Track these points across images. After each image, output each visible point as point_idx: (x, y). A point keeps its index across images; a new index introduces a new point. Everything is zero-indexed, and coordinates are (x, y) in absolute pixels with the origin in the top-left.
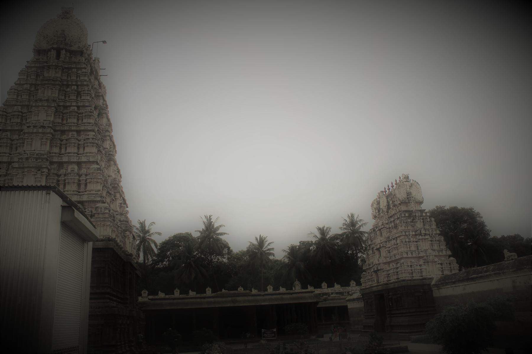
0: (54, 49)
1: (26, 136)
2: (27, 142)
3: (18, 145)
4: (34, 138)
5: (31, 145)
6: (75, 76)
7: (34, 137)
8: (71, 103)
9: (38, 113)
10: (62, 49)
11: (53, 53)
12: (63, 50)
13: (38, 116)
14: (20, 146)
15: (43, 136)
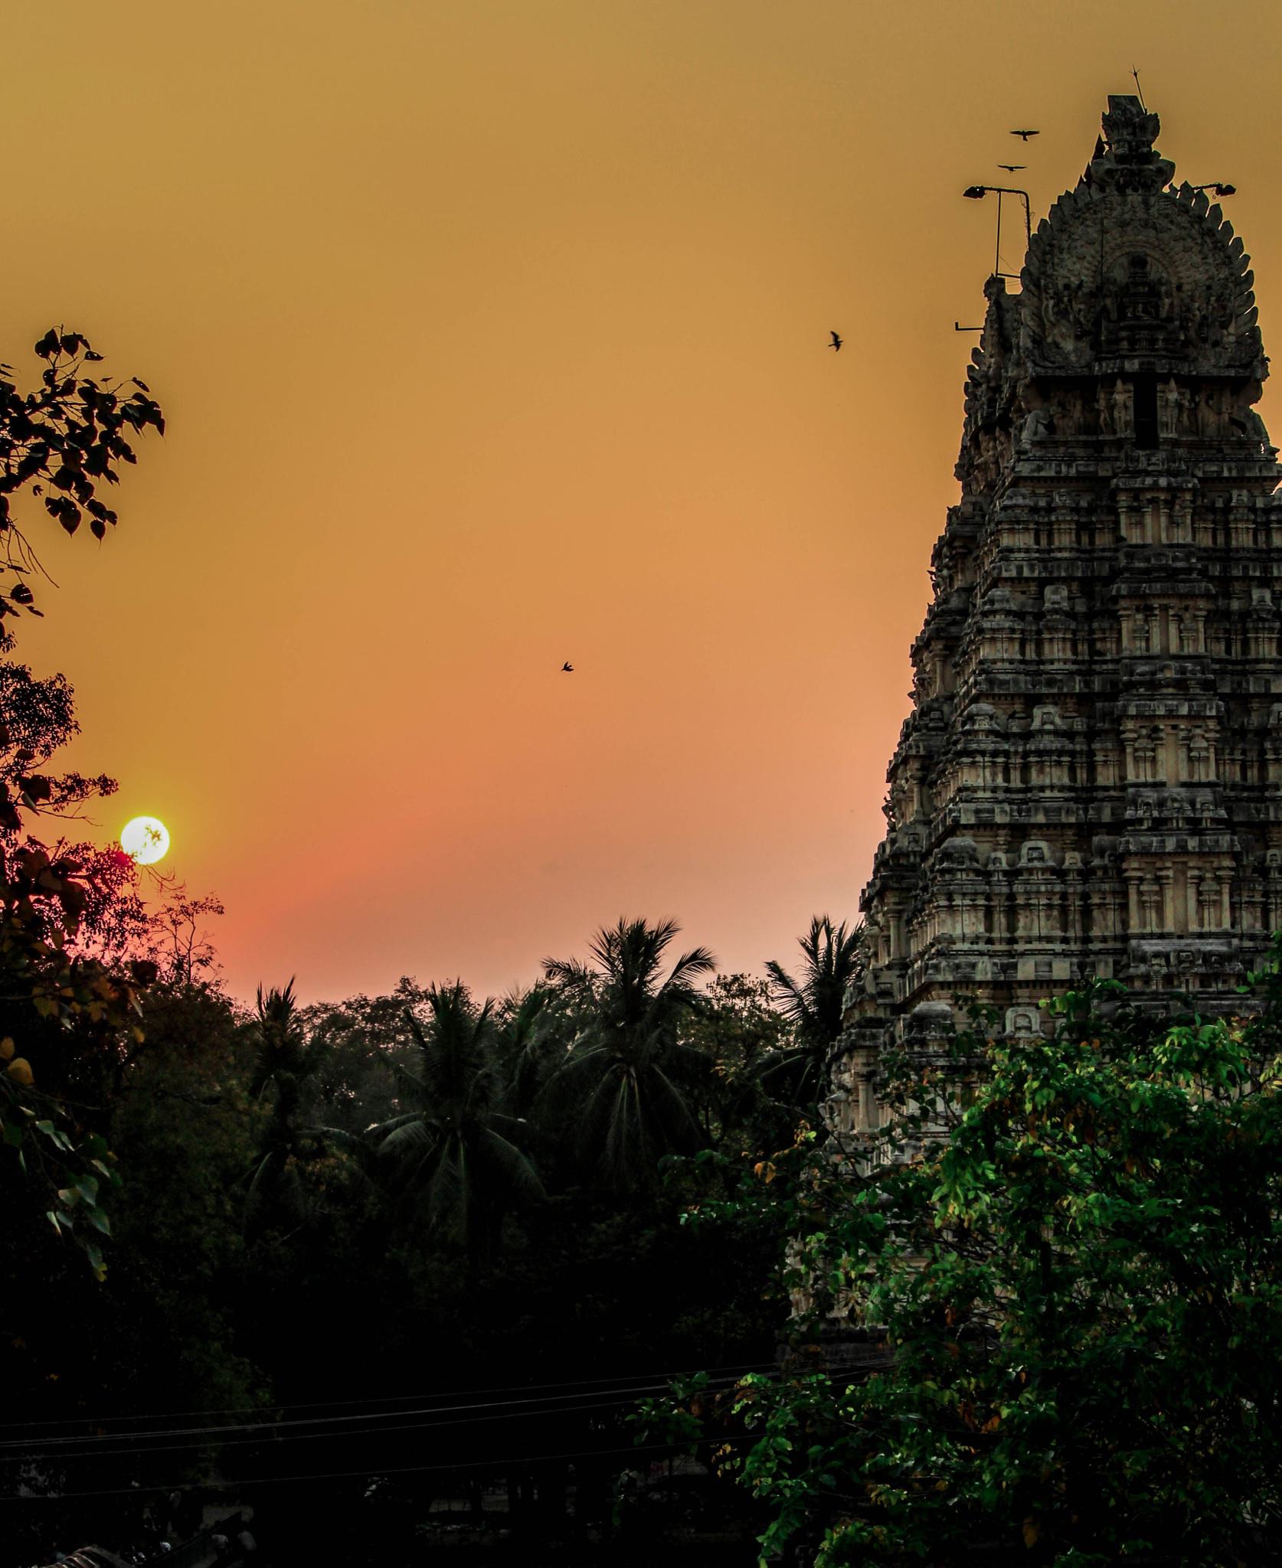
0: (1126, 377)
1: (1134, 869)
2: (1140, 893)
3: (1096, 900)
4: (1167, 877)
5: (1160, 908)
6: (1248, 529)
7: (1170, 873)
8: (1268, 682)
9: (1153, 750)
10: (1165, 379)
11: (1122, 395)
12: (1167, 383)
13: (1154, 760)
14: (1100, 906)
15: (1200, 864)
